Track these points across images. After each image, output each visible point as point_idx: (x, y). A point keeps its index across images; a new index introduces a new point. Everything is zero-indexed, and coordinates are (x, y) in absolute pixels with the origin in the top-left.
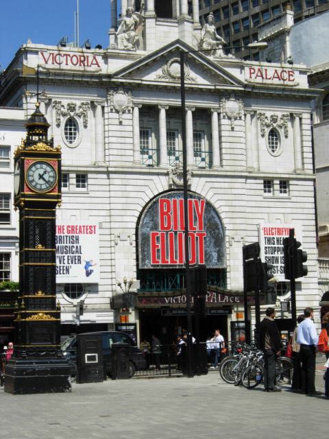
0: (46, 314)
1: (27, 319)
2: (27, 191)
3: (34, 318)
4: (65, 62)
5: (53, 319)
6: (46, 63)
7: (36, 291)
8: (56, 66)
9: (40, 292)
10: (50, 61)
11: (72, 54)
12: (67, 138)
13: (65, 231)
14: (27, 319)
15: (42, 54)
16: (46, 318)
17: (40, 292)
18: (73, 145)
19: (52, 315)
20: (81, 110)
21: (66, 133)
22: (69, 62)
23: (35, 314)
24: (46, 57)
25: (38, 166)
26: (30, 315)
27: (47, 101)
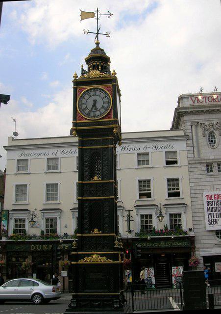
0: (102, 255)
1: (81, 262)
2: (79, 120)
3: (88, 260)
4: (204, 101)
5: (111, 262)
6: (194, 103)
7: (91, 229)
8: (200, 104)
9: (96, 230)
10: (196, 102)
11: (208, 96)
12: (210, 143)
13: (213, 198)
14: (81, 262)
15: (191, 98)
16: (103, 260)
17: (96, 230)
18: (215, 147)
19: (108, 256)
20: (217, 126)
21: (209, 141)
22: (207, 101)
23: (88, 255)
24: (194, 99)
25: (92, 93)
26: (82, 257)
27: (196, 124)
